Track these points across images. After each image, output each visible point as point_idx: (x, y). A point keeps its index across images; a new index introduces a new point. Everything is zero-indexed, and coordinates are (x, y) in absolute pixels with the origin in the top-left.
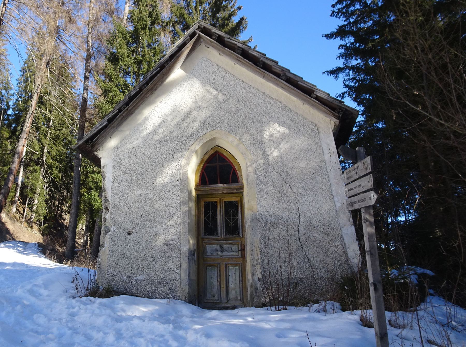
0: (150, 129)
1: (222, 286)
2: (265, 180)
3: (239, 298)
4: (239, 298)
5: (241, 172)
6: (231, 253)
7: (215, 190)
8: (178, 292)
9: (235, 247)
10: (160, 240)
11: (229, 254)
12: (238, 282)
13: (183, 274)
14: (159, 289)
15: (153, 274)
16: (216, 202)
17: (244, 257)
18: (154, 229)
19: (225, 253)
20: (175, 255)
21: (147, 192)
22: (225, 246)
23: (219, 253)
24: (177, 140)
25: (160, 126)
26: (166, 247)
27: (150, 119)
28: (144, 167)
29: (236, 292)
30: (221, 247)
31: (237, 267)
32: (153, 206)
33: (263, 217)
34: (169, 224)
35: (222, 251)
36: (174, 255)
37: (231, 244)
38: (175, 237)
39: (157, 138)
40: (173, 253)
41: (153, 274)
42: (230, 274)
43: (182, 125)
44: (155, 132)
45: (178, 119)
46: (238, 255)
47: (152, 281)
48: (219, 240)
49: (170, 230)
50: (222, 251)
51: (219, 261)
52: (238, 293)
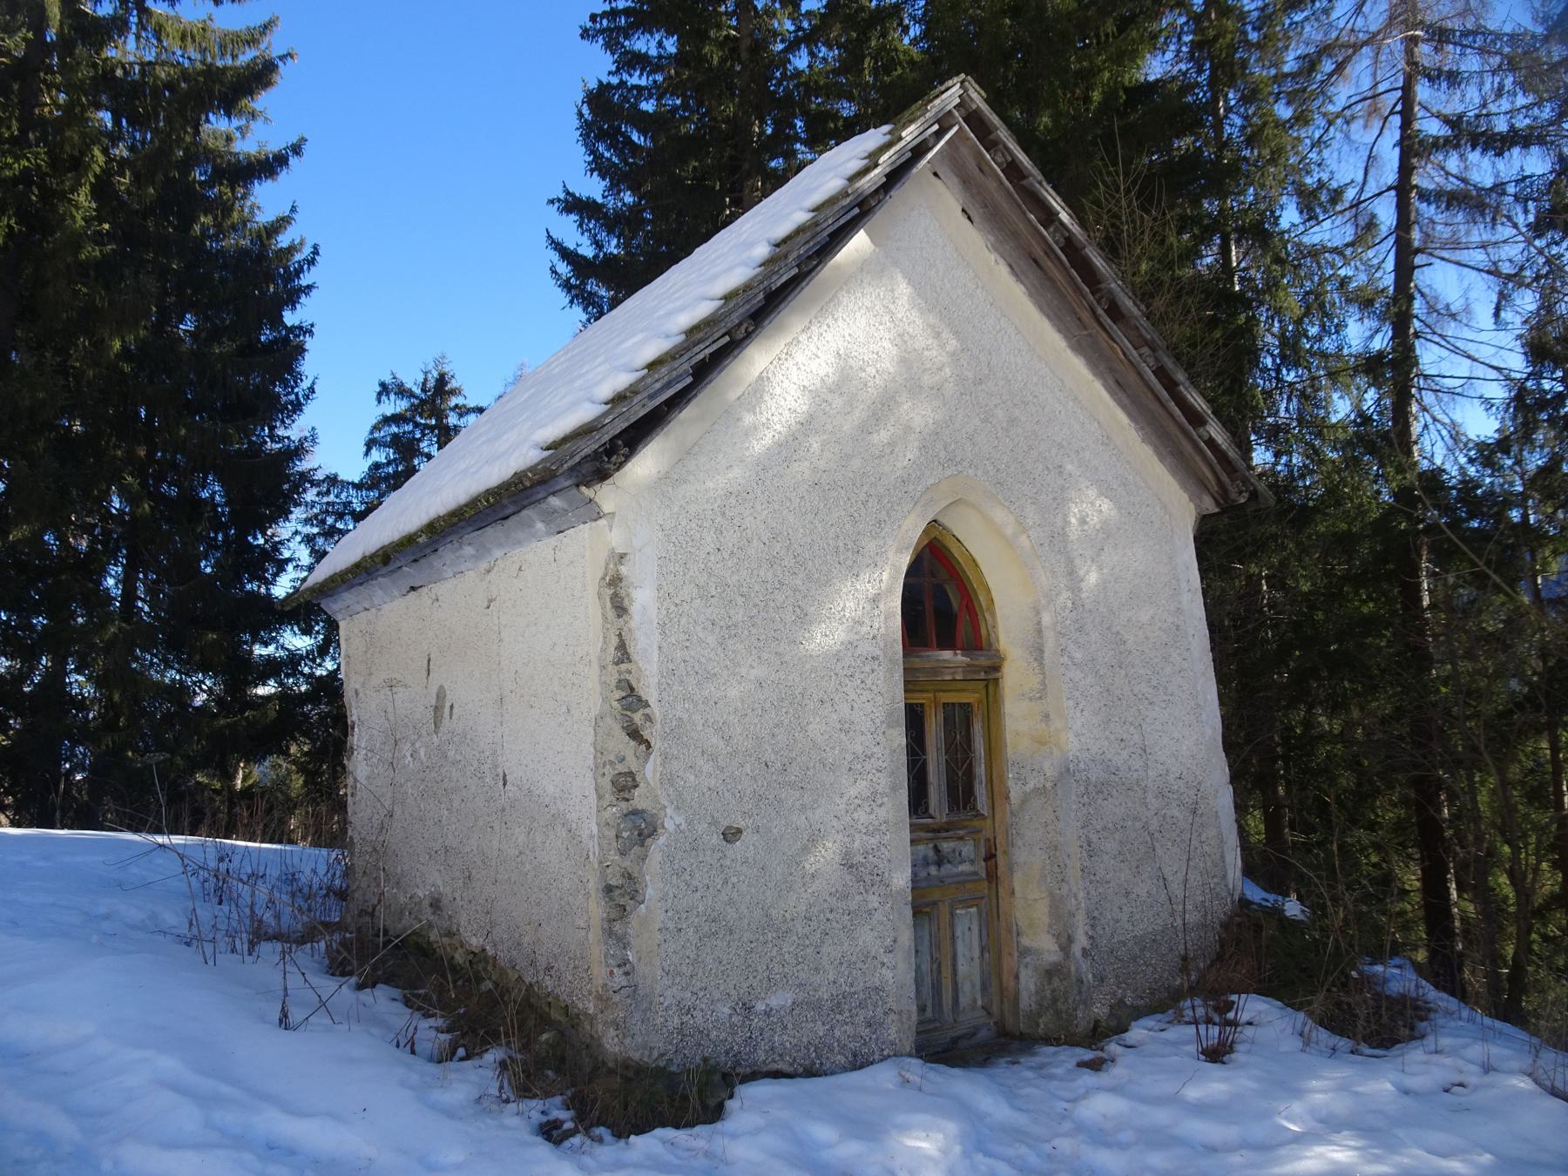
0: (778, 427)
1: (944, 974)
2: (1078, 656)
3: (979, 1003)
4: (979, 1003)
5: (993, 614)
6: (962, 868)
7: (935, 671)
8: (893, 1031)
9: (967, 849)
10: (826, 856)
11: (955, 870)
12: (976, 953)
13: (902, 966)
14: (837, 1033)
15: (816, 979)
16: (922, 705)
17: (992, 876)
18: (809, 813)
19: (947, 869)
20: (876, 905)
21: (781, 675)
22: (946, 846)
23: (933, 870)
24: (865, 488)
25: (807, 425)
26: (848, 877)
27: (778, 391)
28: (770, 575)
29: (973, 986)
30: (937, 850)
31: (973, 910)
32: (803, 730)
33: (1082, 766)
34: (853, 792)
35: (939, 864)
36: (874, 901)
37: (961, 838)
38: (873, 840)
39: (801, 469)
40: (871, 898)
41: (816, 979)
42: (958, 933)
43: (875, 438)
44: (790, 446)
45: (858, 415)
46: (975, 873)
47: (816, 1006)
48: (934, 831)
49: (856, 815)
50: (939, 864)
51: (936, 895)
52: (978, 987)
